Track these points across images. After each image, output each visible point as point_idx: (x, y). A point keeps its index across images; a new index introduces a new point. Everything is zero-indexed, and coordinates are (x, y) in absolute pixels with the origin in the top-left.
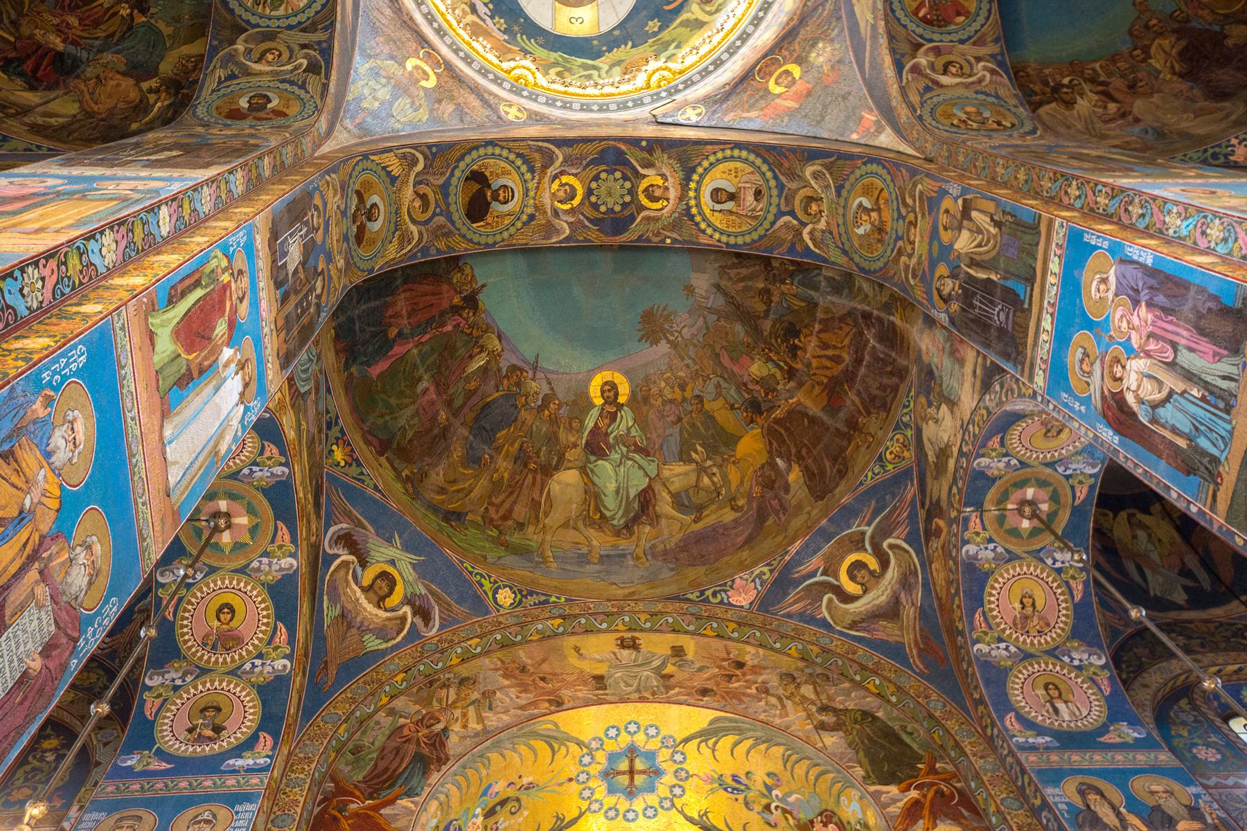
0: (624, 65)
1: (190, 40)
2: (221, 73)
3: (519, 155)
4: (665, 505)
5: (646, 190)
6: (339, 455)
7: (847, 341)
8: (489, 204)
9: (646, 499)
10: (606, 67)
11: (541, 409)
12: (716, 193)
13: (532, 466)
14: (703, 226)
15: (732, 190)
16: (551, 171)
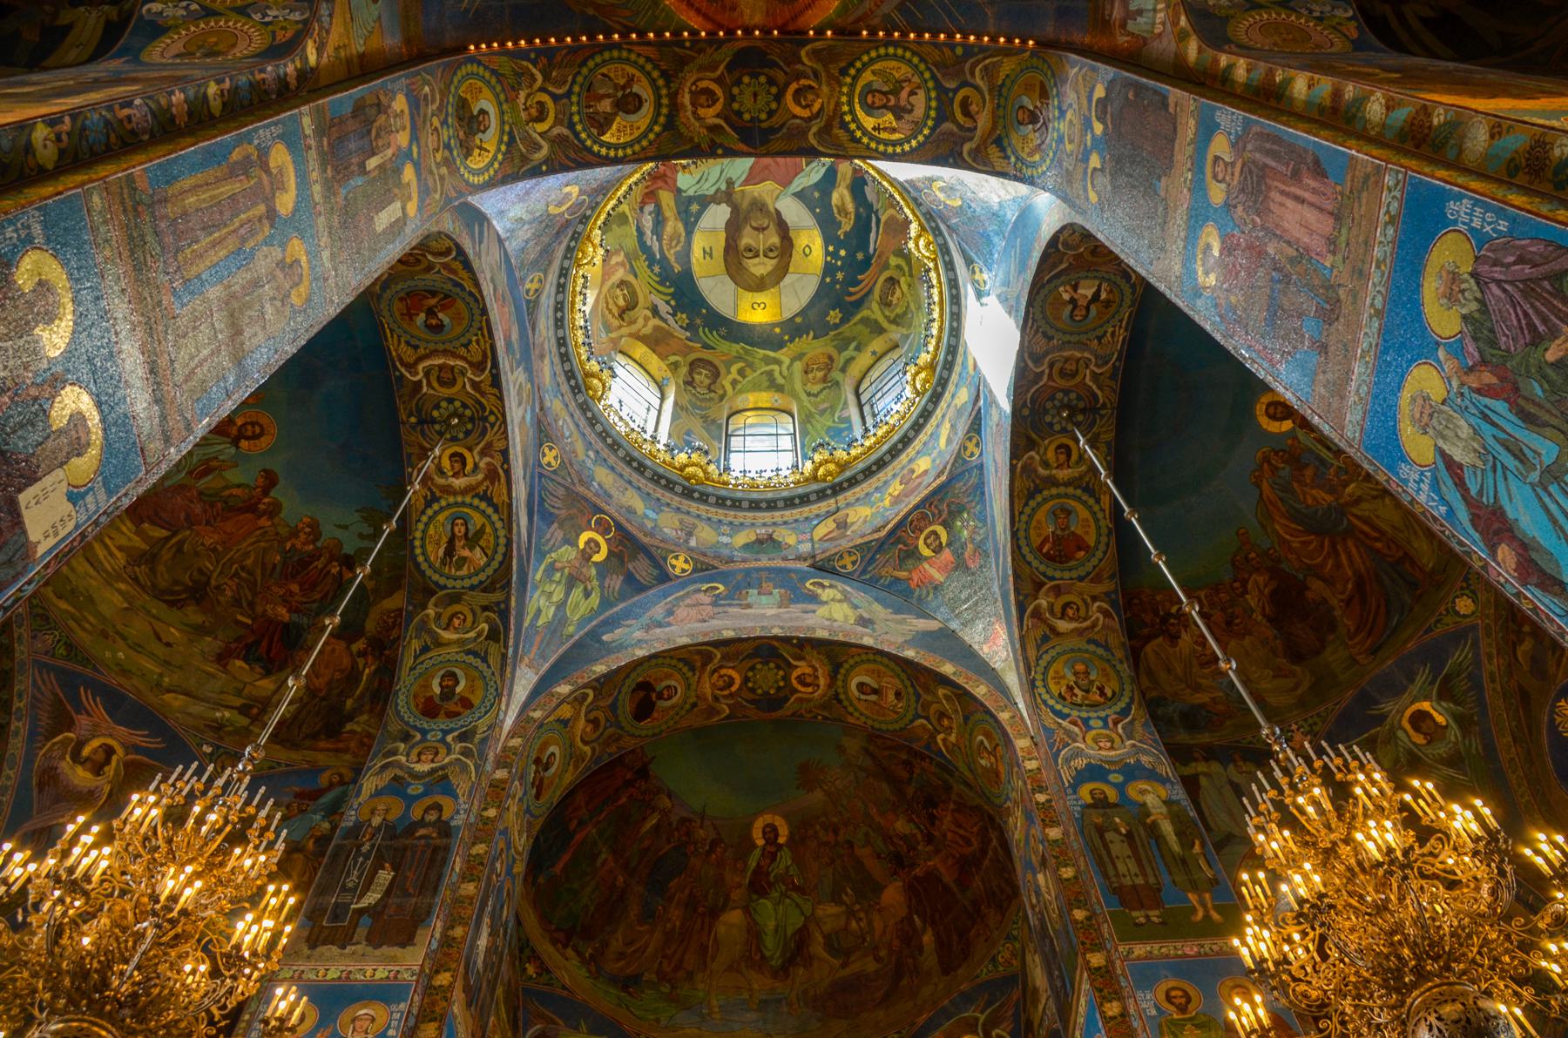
0: (806, 359)
1: (390, 594)
2: (416, 645)
3: (680, 660)
4: (818, 948)
5: (798, 677)
6: (531, 970)
7: (975, 829)
8: (653, 704)
9: (802, 938)
10: (787, 361)
11: (708, 853)
12: (861, 686)
13: (701, 910)
14: (850, 709)
15: (876, 686)
16: (710, 667)
